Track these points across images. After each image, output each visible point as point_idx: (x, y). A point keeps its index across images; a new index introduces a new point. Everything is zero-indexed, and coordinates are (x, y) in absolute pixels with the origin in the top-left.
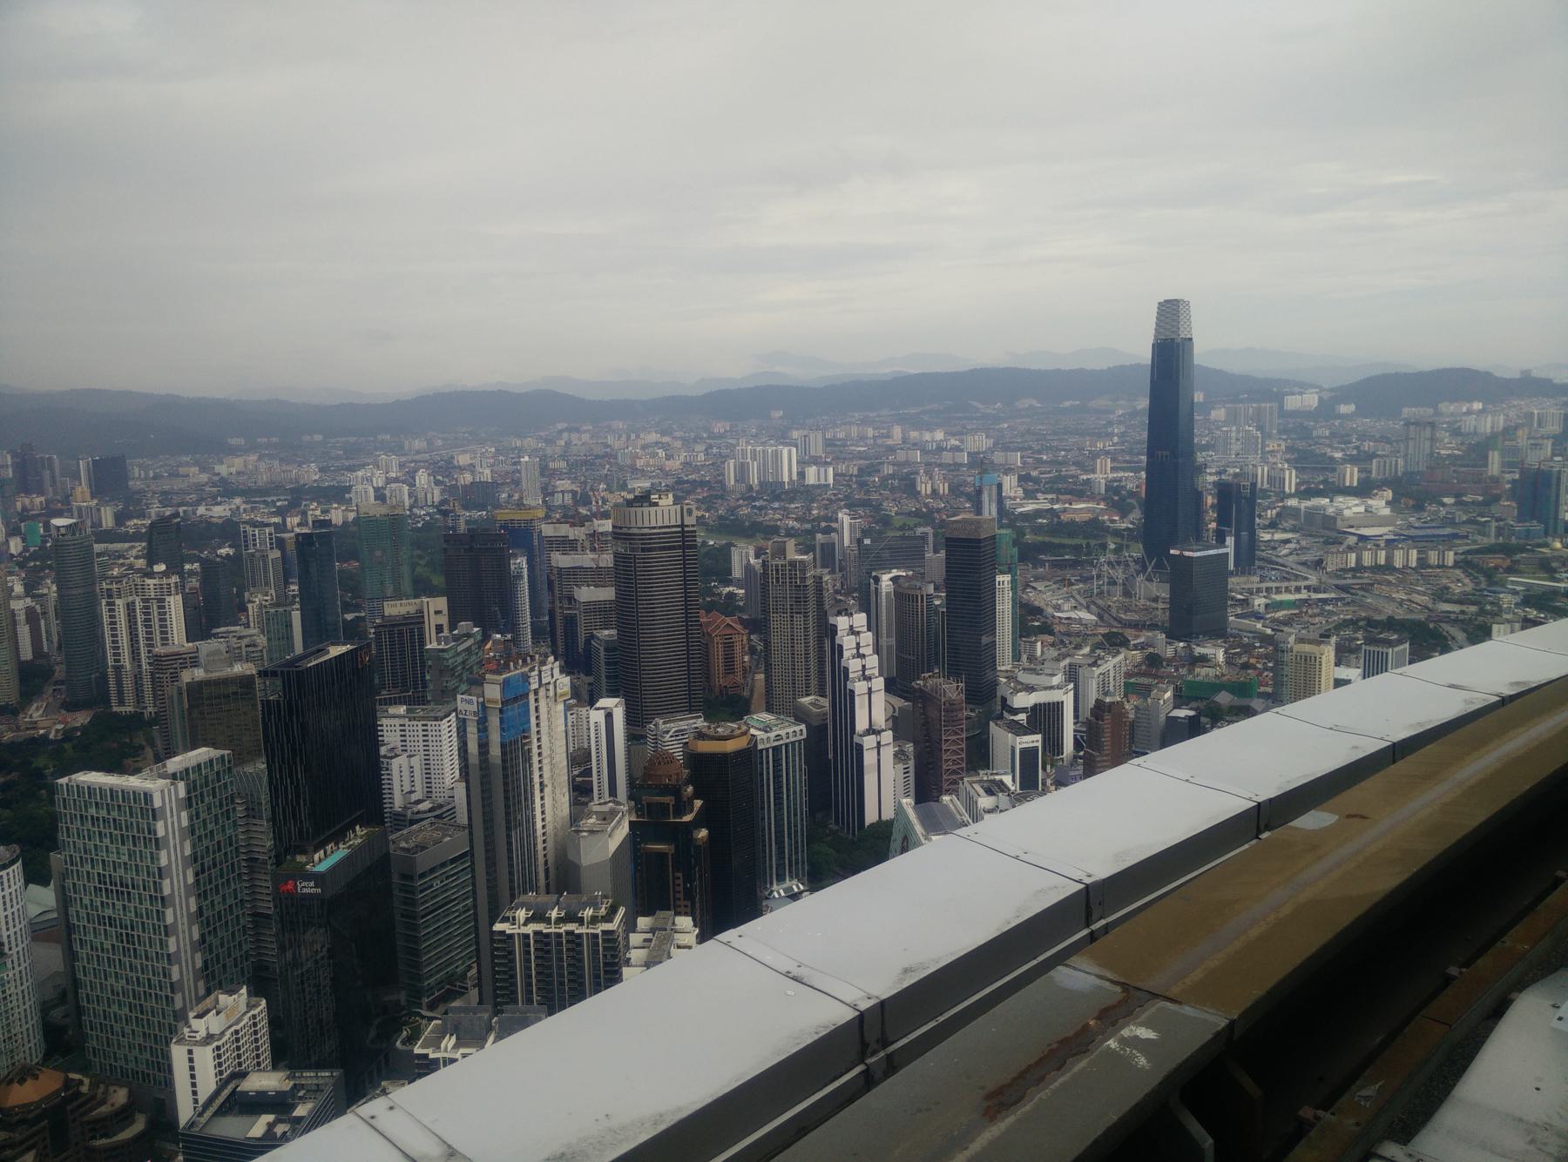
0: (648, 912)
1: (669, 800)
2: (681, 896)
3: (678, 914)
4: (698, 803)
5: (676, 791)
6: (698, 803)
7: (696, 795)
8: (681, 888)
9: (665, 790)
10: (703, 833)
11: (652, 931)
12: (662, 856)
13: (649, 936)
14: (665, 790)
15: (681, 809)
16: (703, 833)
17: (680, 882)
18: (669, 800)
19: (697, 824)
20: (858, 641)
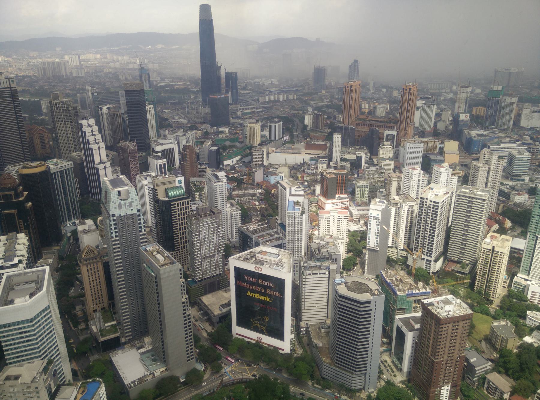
0: (3, 235)
1: (12, 193)
2: (23, 228)
3: (18, 233)
4: (26, 193)
5: (15, 189)
6: (26, 193)
7: (24, 190)
8: (23, 226)
9: (10, 189)
10: (30, 204)
11: (7, 240)
12: (12, 215)
13: (6, 242)
14: (10, 189)
15: (17, 195)
16: (30, 204)
17: (22, 223)
18: (12, 193)
19: (27, 200)
20: (89, 126)
